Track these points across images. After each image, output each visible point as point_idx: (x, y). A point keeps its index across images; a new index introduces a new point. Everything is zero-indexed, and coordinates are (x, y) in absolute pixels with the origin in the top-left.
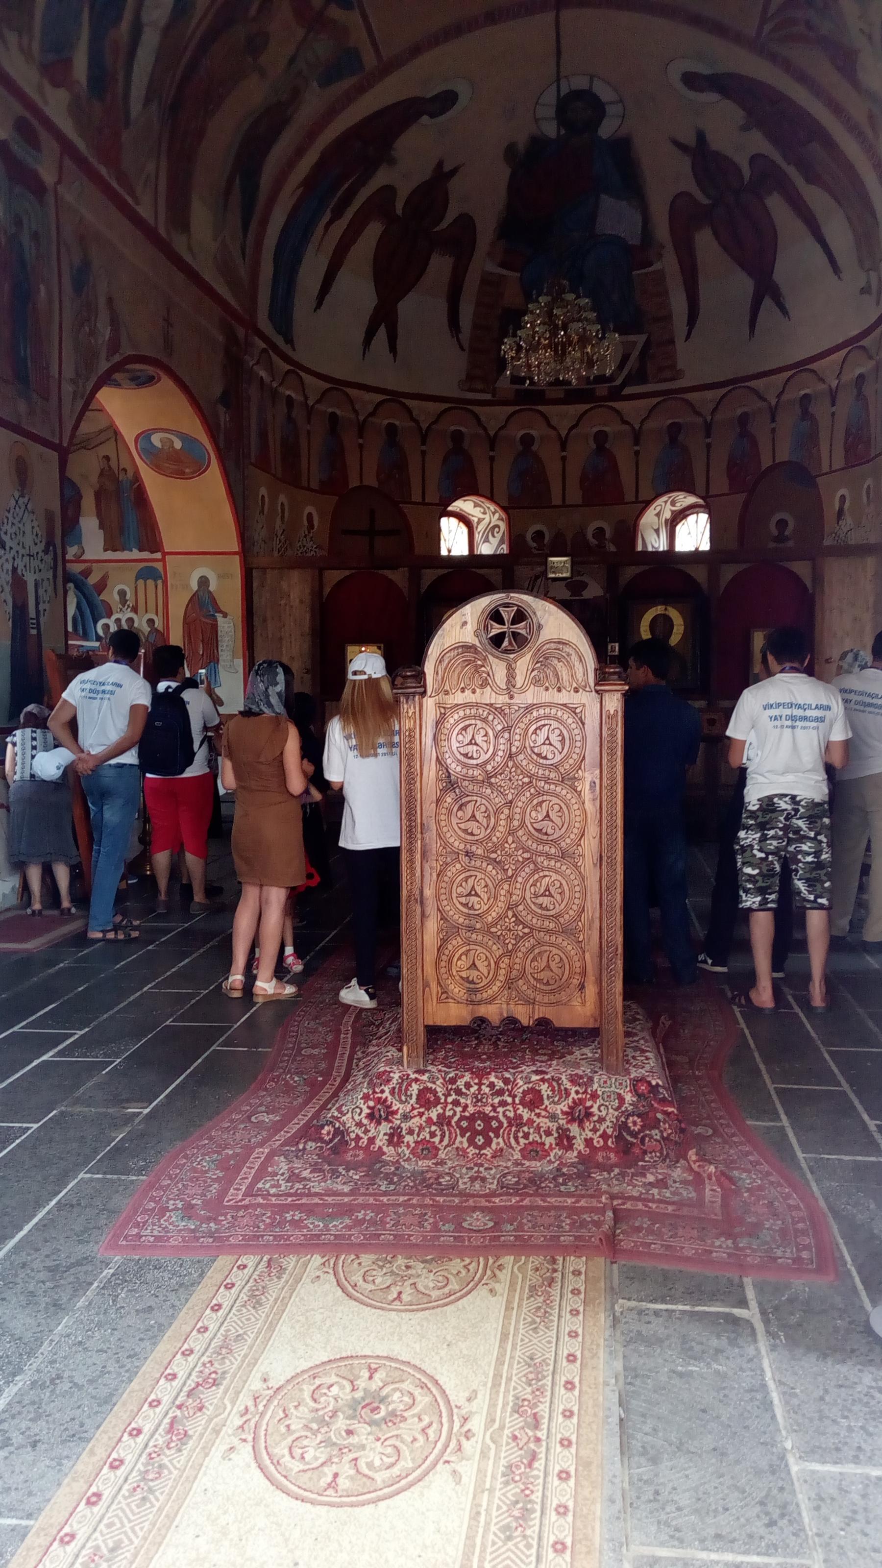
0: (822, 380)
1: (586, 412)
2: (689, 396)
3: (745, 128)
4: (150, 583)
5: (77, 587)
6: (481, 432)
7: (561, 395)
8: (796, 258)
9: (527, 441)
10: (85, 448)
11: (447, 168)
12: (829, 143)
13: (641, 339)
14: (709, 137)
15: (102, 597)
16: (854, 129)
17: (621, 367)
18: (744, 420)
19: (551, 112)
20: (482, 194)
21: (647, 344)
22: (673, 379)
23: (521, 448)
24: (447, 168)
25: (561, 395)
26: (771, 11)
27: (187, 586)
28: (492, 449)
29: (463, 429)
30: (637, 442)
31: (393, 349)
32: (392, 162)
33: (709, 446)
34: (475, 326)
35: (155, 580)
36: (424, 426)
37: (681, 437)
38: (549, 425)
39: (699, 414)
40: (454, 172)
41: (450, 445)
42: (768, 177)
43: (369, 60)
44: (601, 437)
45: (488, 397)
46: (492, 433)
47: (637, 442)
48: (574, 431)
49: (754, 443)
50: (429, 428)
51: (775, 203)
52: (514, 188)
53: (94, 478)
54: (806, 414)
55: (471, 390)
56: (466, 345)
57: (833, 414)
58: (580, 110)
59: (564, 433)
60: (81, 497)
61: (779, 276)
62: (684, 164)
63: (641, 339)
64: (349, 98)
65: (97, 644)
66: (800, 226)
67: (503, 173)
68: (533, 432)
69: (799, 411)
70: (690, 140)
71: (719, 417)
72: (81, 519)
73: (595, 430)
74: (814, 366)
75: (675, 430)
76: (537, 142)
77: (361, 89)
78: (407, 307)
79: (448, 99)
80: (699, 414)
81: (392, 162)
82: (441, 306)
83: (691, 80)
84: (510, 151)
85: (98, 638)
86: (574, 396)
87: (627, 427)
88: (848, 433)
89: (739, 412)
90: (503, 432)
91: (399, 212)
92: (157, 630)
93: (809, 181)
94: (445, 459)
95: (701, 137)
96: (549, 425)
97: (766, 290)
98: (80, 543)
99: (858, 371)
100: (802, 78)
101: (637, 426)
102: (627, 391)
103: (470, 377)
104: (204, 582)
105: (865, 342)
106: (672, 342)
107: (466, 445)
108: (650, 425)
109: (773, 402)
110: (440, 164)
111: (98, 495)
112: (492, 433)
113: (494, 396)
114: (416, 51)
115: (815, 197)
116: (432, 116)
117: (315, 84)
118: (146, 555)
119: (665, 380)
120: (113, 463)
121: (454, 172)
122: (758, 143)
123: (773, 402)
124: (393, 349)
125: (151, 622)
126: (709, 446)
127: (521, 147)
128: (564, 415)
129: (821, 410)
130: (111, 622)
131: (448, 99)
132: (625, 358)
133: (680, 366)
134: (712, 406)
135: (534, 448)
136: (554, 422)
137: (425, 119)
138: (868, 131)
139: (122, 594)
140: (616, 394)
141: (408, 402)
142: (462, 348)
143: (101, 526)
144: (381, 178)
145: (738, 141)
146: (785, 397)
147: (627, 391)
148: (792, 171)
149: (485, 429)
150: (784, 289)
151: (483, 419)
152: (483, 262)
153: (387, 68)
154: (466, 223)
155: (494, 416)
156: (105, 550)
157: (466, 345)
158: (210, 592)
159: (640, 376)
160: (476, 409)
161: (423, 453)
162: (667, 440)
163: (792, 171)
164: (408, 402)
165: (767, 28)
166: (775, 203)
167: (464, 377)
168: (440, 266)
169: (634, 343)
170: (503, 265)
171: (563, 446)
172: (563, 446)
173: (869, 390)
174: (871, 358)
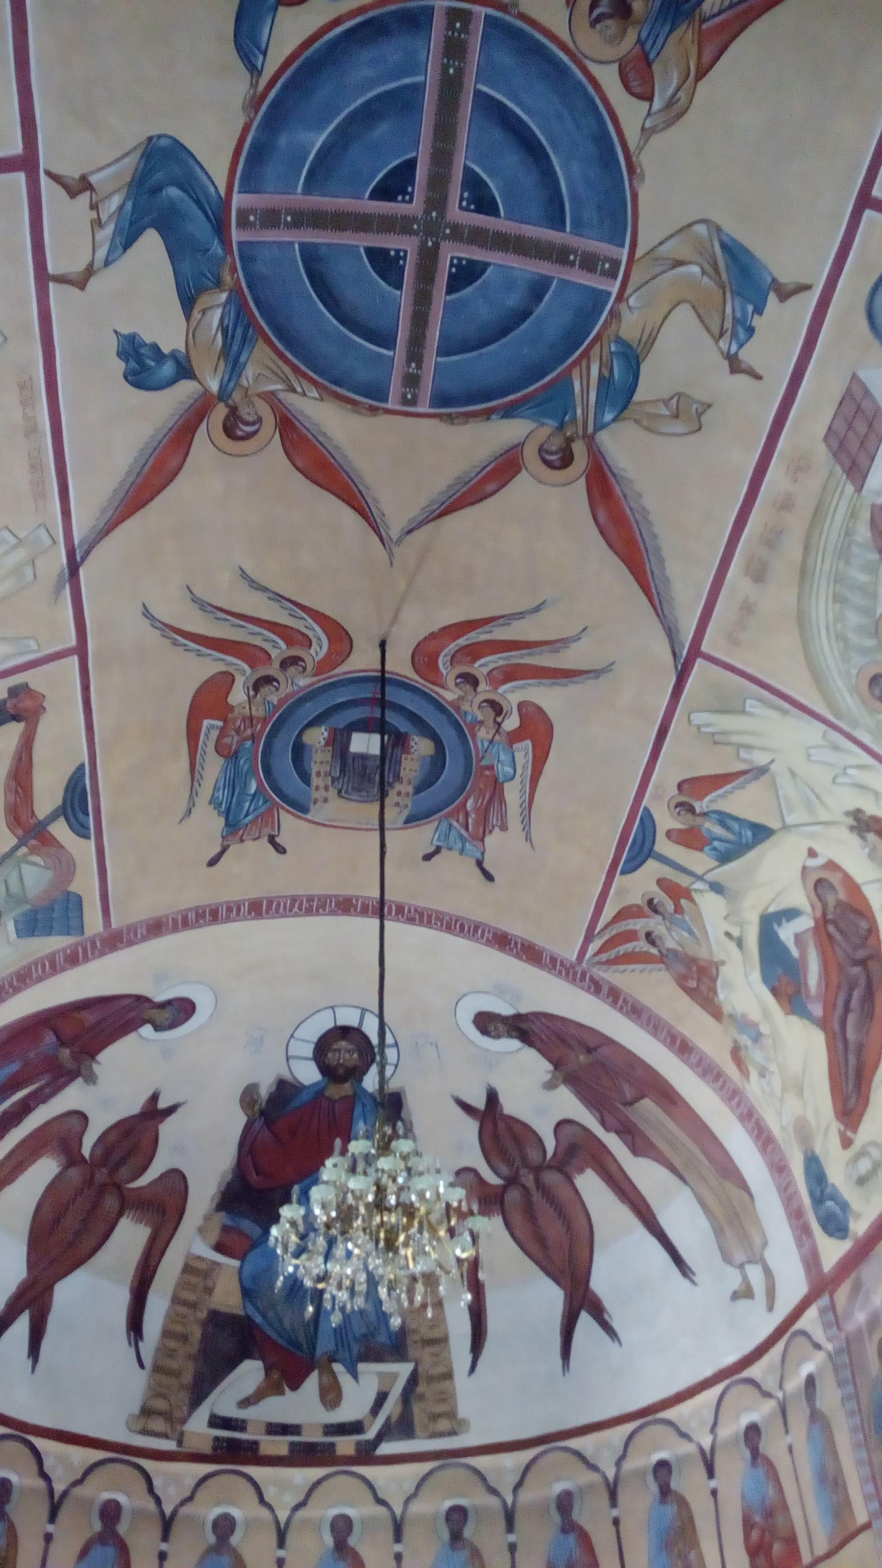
0: (684, 1435)
1: (319, 1482)
2: (480, 1462)
3: (550, 1086)
6: (151, 1505)
7: (284, 1451)
8: (621, 1259)
9: (224, 1526)
11: (162, 1104)
12: (668, 1097)
13: (404, 1370)
14: (502, 1098)
16: (708, 1071)
17: (375, 1410)
18: (565, 1503)
19: (308, 1050)
20: (203, 1148)
21: (413, 1380)
22: (453, 1433)
23: (212, 1539)
24: (162, 1104)
25: (284, 1451)
26: (600, 925)
28: (165, 1538)
29: (122, 1499)
30: (398, 1536)
31: (34, 1350)
32: (91, 1079)
33: (512, 1548)
34: (166, 1333)
36: (59, 1488)
37: (467, 1532)
38: (262, 1500)
39: (494, 1491)
40: (171, 1110)
41: (97, 1526)
42: (578, 1149)
43: (93, 922)
44: (342, 1527)
45: (169, 1445)
46: (168, 1509)
47: (398, 1536)
48: (302, 1513)
49: (585, 1540)
50: (65, 1494)
51: (589, 1185)
52: (248, 1145)
54: (665, 1492)
55: (145, 1432)
56: (148, 1361)
57: (714, 1493)
58: (346, 1052)
59: (283, 1516)
61: (600, 1282)
62: (470, 1128)
63: (404, 1370)
64: (52, 966)
66: (624, 1214)
67: (235, 1122)
68: (235, 1512)
69: (654, 1488)
70: (480, 1103)
71: (526, 1496)
73: (334, 1512)
74: (670, 1414)
75: (457, 1517)
76: (285, 1089)
77: (73, 959)
78: (69, 1292)
79: (183, 1009)
80: (494, 1491)
81: (91, 1079)
82: (123, 1297)
83: (486, 1023)
84: (249, 1096)
86: (307, 1454)
87: (381, 1510)
88: (748, 1524)
89: (558, 1488)
90: (185, 1510)
91: (86, 1151)
93: (635, 1151)
94: (84, 1552)
95: (492, 1097)
96: (262, 1500)
97: (581, 1302)
99: (745, 1420)
100: (635, 1011)
101: (398, 1511)
102: (386, 1448)
103: (146, 1412)
105: (754, 1371)
106: (449, 1375)
107: (122, 1528)
108: (416, 1508)
109: (611, 1473)
110: (155, 1098)
112: (168, 1509)
113: (180, 1443)
114: (156, 928)
115: (645, 1174)
116: (157, 1028)
117: (11, 926)
119: (441, 1435)
121: (171, 1110)
122: (567, 1104)
123: (611, 1473)
124: (34, 1350)
126: (512, 1548)
127: (264, 1092)
128: (286, 1483)
129: (691, 1484)
131: (183, 1009)
132: (381, 1398)
133: (462, 1413)
134: (515, 1478)
135: (234, 1540)
136: (270, 1494)
137: (147, 1030)
138: (731, 1070)
140: (366, 1455)
141: (40, 1443)
142: (142, 1365)
144: (71, 1097)
145: (541, 1101)
146: (629, 1465)
147: (386, 1448)
148: (613, 1142)
149: (158, 1501)
150: (608, 1303)
151: (157, 1483)
152: (192, 1240)
153: (114, 941)
154: (176, 1183)
155: (175, 1479)
157: (148, 1361)
159: (403, 1426)
160: (147, 1464)
161: (48, 1538)
162: (446, 1535)
163: (613, 1142)
164: (40, 1443)
165: (593, 948)
166: (589, 1185)
167: (136, 1410)
168: (130, 1236)
169: (395, 1376)
170: (219, 1248)
171: (281, 1543)
172: (281, 1543)
173: (774, 1446)
174: (767, 1395)
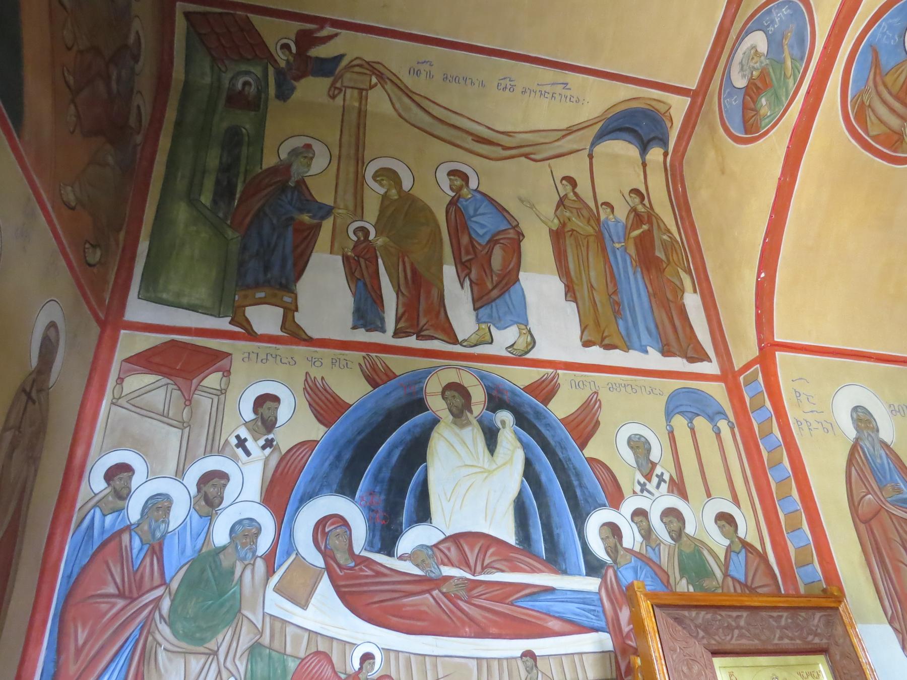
4: (700, 423)
5: (522, 421)
10: (526, 156)
15: (591, 451)
27: (830, 427)
35: (711, 419)
53: (548, 208)
60: (520, 235)
65: (592, 584)
72: (522, 275)
85: (594, 567)
92: (745, 545)
98: (522, 321)
104: (863, 419)
111: (558, 237)
118: (677, 364)
120: (584, 188)
125: (725, 520)
130: (622, 517)
139: (639, 446)
143: (571, 292)
156: (587, 344)
158: (885, 445)
